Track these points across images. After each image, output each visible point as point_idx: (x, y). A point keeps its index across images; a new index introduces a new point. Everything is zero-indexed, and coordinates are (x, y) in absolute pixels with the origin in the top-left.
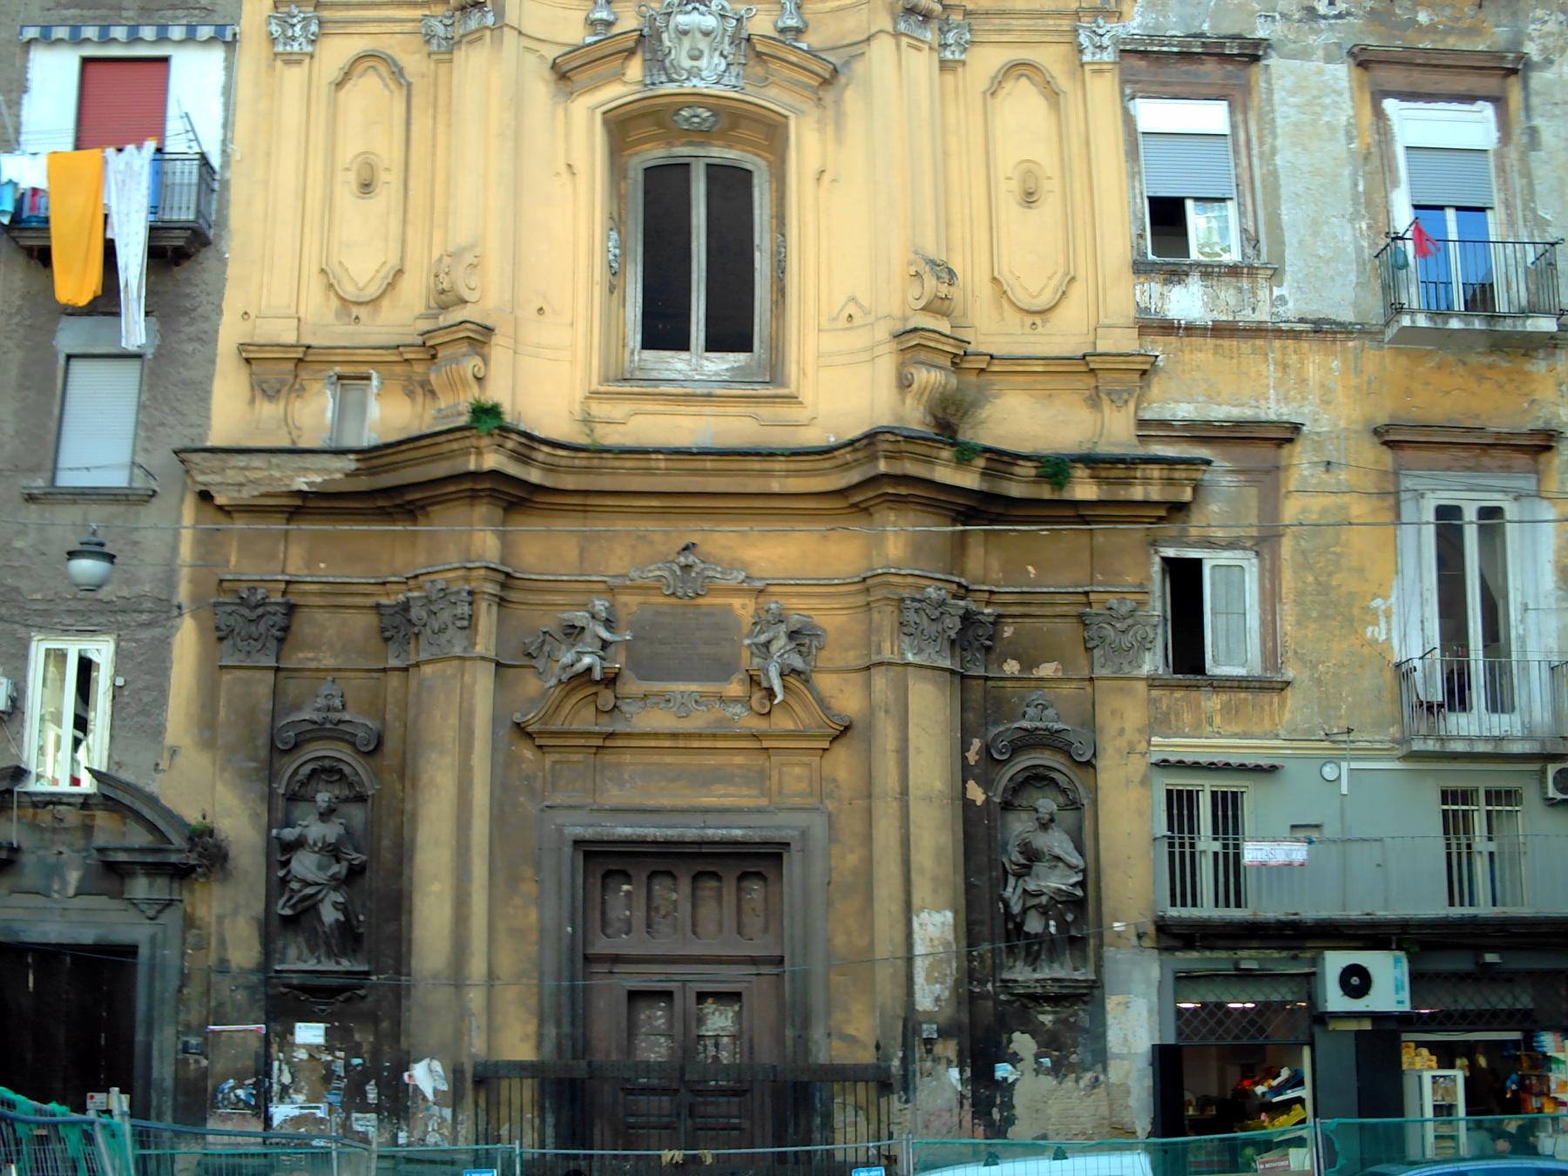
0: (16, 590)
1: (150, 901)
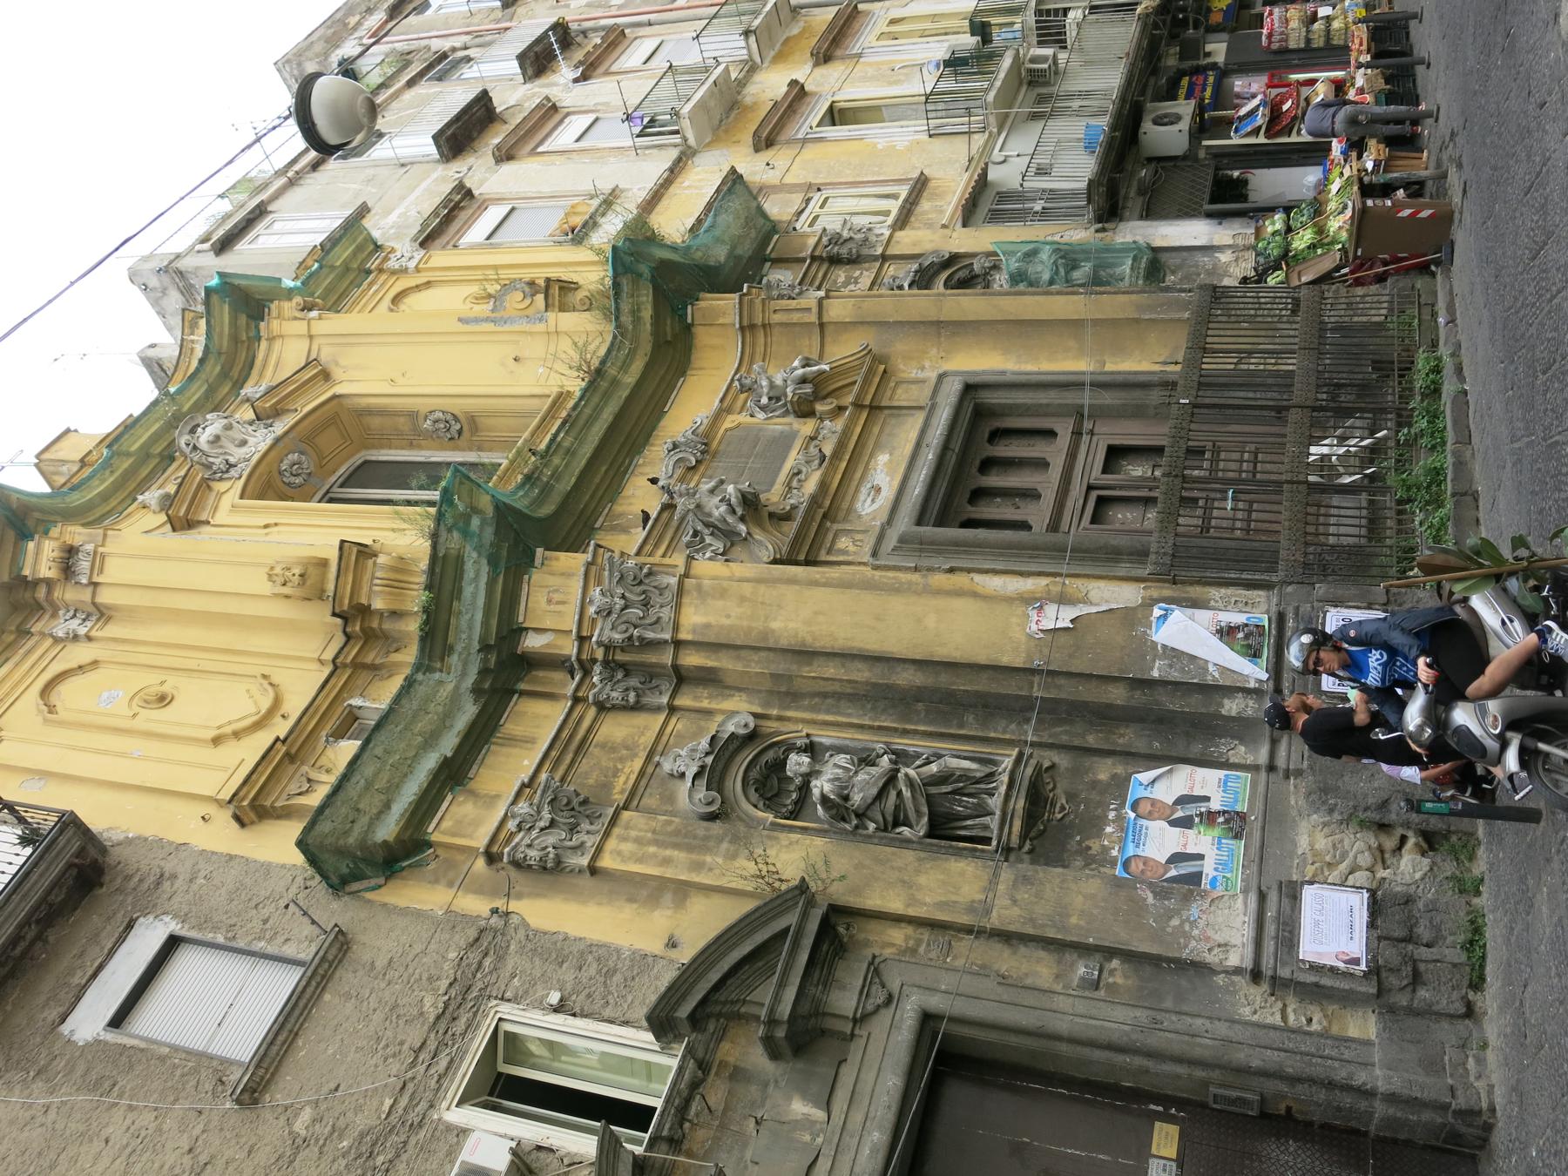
0: (362, 1135)
1: (865, 993)
